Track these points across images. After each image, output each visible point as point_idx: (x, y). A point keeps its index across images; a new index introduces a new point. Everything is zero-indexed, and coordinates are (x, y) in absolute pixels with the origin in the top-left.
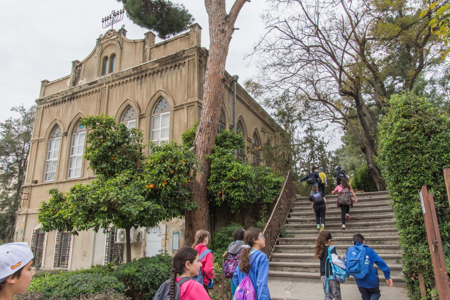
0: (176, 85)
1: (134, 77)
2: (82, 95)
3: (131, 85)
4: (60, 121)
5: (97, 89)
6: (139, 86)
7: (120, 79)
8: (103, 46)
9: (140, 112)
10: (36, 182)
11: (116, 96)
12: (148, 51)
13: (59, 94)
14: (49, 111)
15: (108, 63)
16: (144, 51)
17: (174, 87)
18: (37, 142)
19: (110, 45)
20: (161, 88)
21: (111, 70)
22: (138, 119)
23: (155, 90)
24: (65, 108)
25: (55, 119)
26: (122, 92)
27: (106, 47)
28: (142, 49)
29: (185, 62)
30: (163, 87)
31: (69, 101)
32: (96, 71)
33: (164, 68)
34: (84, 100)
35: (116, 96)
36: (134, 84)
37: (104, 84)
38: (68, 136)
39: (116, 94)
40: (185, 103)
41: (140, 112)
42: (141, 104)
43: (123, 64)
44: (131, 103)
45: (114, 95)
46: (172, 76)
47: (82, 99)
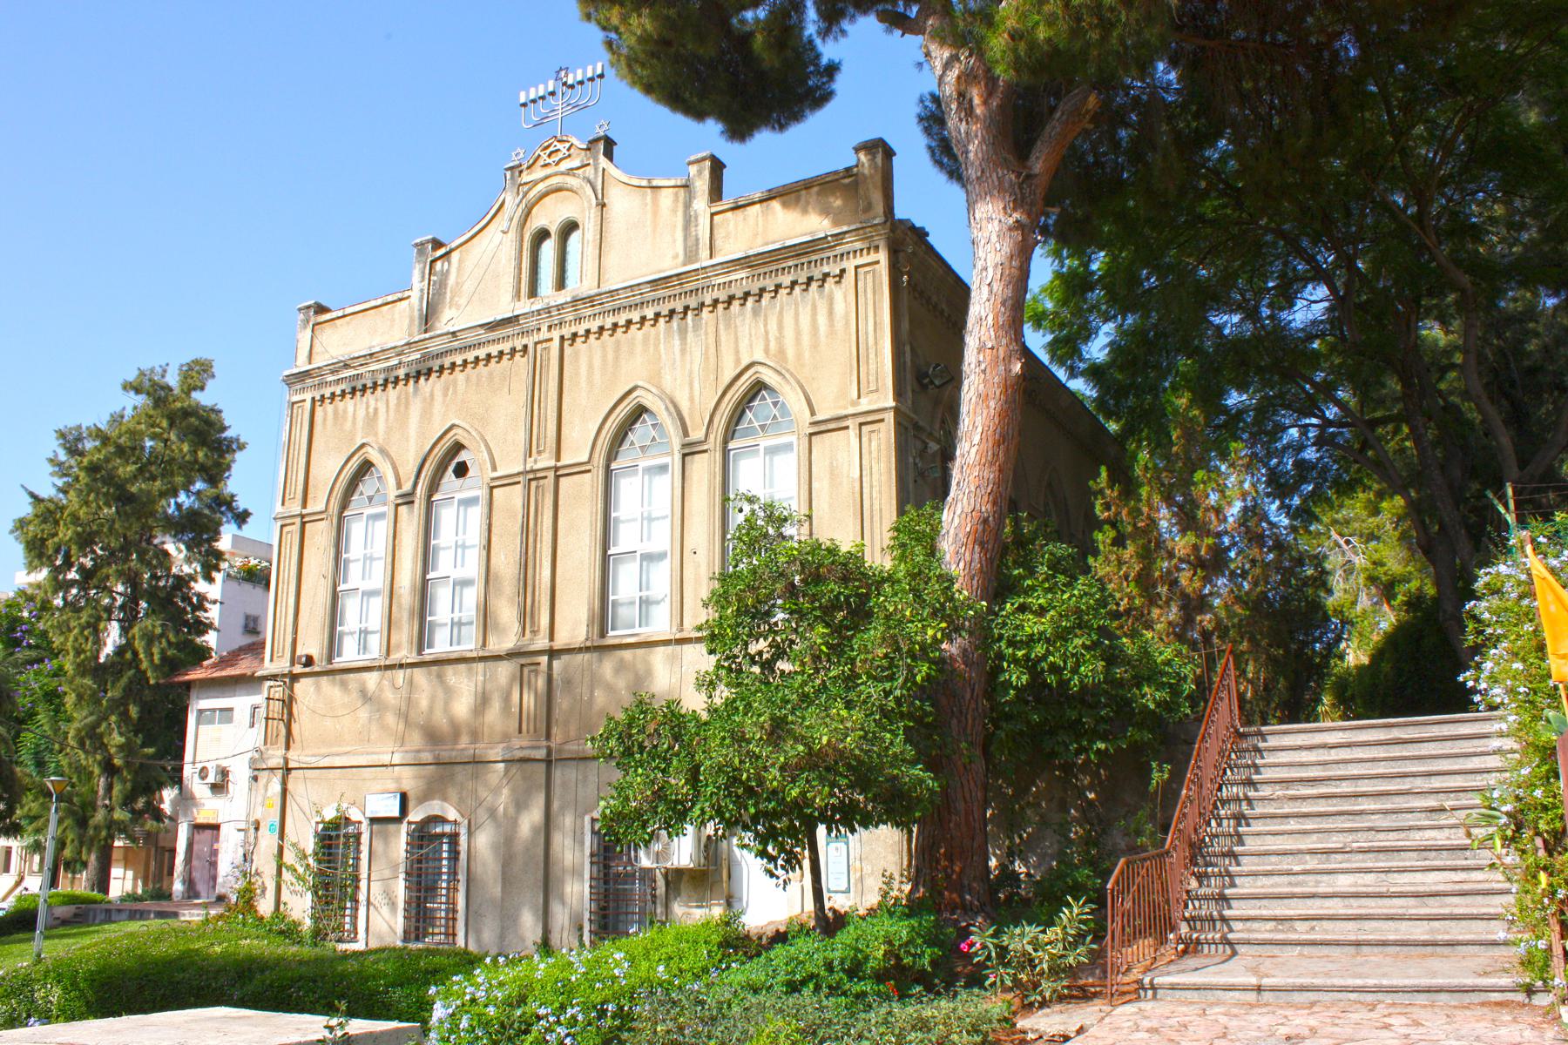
0: (815, 346)
1: (657, 309)
2: (459, 362)
3: (646, 339)
4: (383, 452)
6: (677, 342)
8: (531, 194)
9: (686, 434)
10: (309, 661)
12: (704, 222)
14: (336, 412)
15: (549, 249)
16: (689, 221)
17: (807, 354)
18: (298, 521)
19: (559, 190)
20: (759, 356)
21: (561, 284)
22: (678, 457)
23: (738, 361)
24: (398, 405)
25: (363, 446)
26: (610, 356)
28: (680, 213)
29: (843, 271)
30: (767, 351)
31: (412, 382)
32: (508, 282)
33: (770, 283)
34: (468, 379)
36: (658, 335)
37: (544, 328)
38: (416, 505)
39: (590, 366)
40: (851, 410)
41: (686, 434)
43: (611, 260)
44: (649, 401)
46: (797, 314)
47: (459, 375)
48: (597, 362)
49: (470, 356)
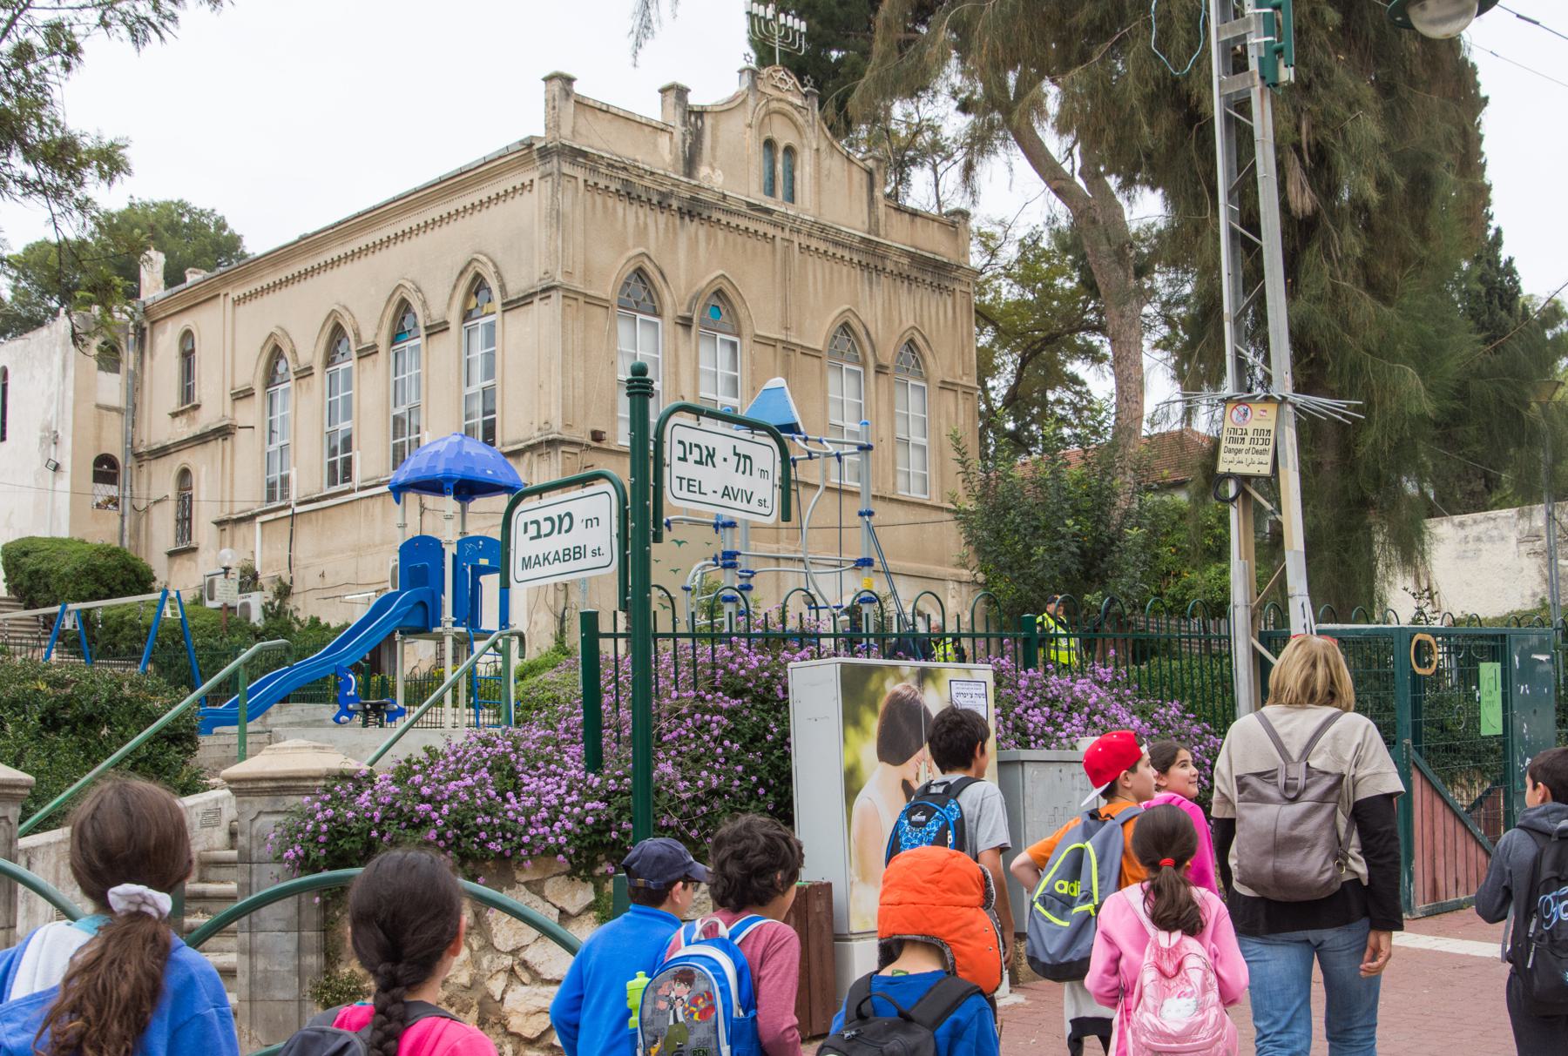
5: (771, 231)
7: (826, 240)
11: (815, 283)
13: (652, 173)
27: (776, 112)
35: (815, 283)
42: (873, 336)
45: (811, 277)
47: (720, 235)
48: (819, 276)
49: (734, 221)
